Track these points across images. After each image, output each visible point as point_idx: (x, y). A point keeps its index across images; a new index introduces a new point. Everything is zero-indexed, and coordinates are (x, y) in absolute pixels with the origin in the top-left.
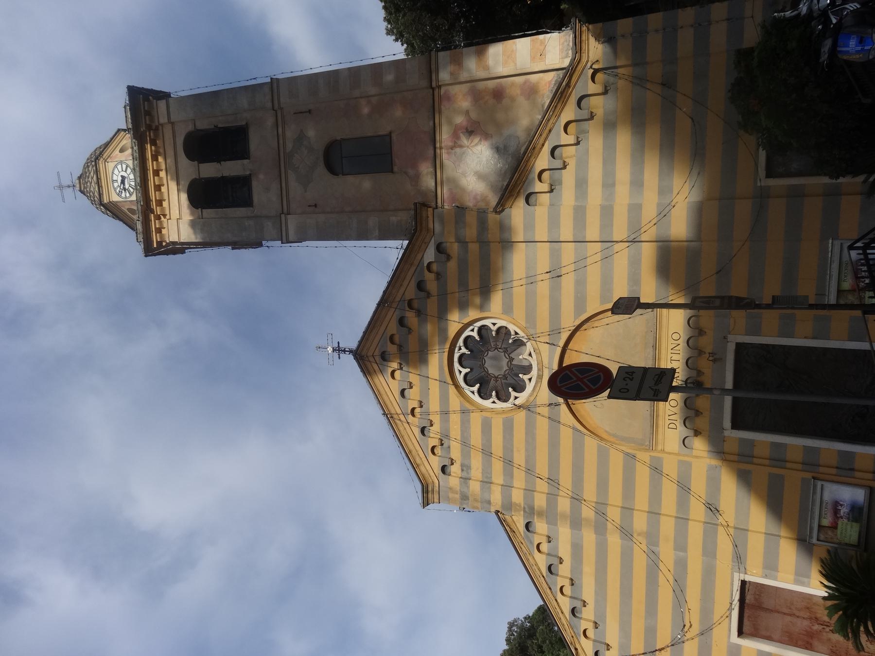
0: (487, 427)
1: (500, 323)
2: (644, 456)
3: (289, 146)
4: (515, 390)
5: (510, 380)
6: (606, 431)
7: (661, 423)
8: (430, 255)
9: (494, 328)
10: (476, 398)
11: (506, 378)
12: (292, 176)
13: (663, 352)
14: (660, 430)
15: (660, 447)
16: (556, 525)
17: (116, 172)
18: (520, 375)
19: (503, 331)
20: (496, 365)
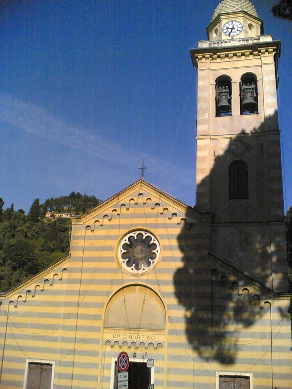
0: (110, 248)
2: (99, 323)
4: (127, 262)
5: (132, 259)
6: (111, 306)
7: (116, 331)
9: (155, 251)
10: (123, 242)
11: (132, 257)
13: (147, 332)
14: (113, 331)
15: (105, 331)
17: (238, 24)
18: (134, 265)
19: (153, 256)
20: (138, 250)
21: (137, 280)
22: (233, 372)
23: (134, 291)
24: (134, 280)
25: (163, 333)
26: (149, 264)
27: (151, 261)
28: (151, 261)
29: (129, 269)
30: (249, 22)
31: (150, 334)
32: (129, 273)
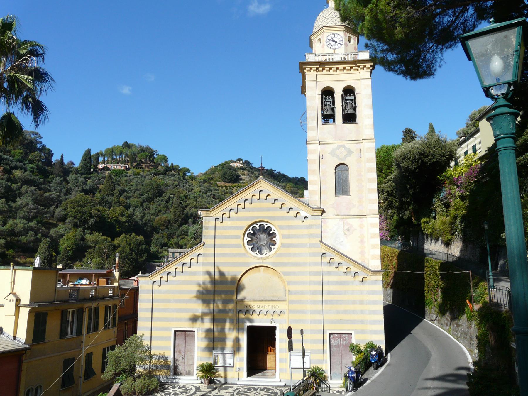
1: (278, 242)
3: (347, 146)
4: (252, 248)
5: (256, 246)
8: (303, 214)
12: (335, 146)
16: (203, 266)
21: (262, 263)
22: (346, 330)
23: (260, 271)
24: (259, 263)
25: (285, 303)
26: (270, 249)
27: (272, 247)
28: (272, 247)
29: (254, 254)
30: (348, 35)
31: (274, 304)
32: (253, 258)
